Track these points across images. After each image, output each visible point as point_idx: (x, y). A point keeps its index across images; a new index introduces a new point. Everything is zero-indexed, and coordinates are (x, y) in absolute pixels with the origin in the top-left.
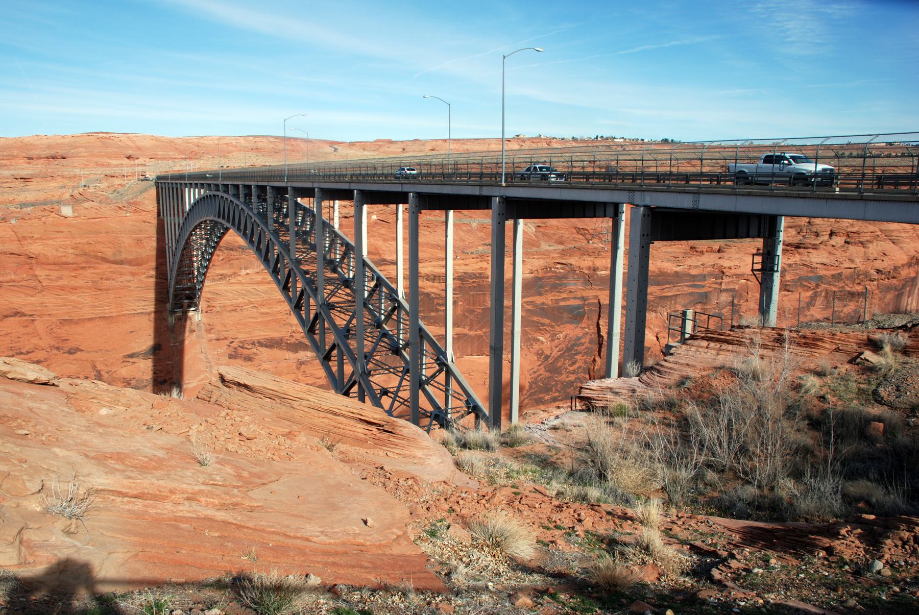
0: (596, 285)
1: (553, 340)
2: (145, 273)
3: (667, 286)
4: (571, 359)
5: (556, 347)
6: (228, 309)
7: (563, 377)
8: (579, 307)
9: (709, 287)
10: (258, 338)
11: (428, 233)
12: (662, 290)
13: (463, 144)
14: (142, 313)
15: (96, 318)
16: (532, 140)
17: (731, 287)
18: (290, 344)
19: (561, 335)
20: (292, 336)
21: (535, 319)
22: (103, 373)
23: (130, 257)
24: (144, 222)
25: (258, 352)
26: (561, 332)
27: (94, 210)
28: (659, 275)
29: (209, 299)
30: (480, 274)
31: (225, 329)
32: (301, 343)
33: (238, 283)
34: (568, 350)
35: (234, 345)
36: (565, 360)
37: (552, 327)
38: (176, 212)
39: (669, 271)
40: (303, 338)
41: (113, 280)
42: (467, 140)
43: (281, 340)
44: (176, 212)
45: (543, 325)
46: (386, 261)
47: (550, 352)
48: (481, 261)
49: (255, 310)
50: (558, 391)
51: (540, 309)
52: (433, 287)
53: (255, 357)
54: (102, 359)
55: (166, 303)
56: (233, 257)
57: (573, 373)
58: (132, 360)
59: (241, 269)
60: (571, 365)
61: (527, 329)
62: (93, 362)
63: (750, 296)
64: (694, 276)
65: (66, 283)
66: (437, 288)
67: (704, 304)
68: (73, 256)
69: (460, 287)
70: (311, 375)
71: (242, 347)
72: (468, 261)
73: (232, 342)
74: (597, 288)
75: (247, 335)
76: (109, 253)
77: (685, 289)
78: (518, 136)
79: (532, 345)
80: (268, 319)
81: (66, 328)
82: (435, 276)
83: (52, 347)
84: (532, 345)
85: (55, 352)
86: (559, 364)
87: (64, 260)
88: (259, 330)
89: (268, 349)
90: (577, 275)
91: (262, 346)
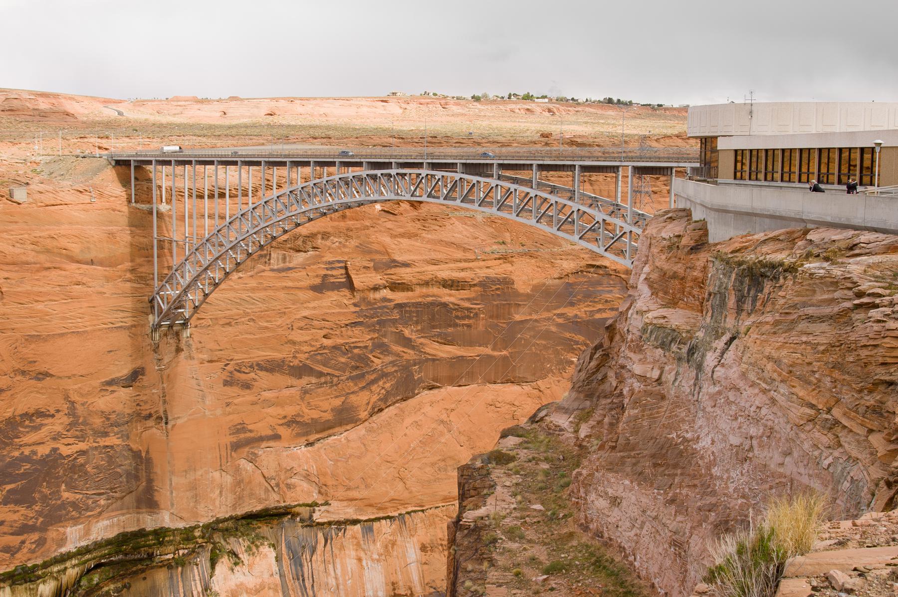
2: (120, 277)
6: (221, 323)
10: (257, 359)
11: (438, 227)
15: (68, 333)
18: (292, 367)
20: (295, 357)
21: (568, 335)
24: (114, 210)
30: (505, 278)
31: (219, 348)
32: (305, 365)
33: (231, 290)
40: (307, 359)
41: (84, 284)
43: (283, 362)
45: (577, 343)
48: (505, 262)
49: (251, 323)
52: (450, 295)
53: (253, 383)
54: (76, 387)
58: (110, 389)
61: (559, 348)
62: (66, 390)
65: (29, 288)
68: (33, 253)
69: (482, 295)
70: (317, 407)
71: (239, 371)
72: (490, 263)
73: (226, 365)
75: (249, 356)
76: (75, 248)
79: (564, 369)
80: (268, 335)
81: (33, 346)
82: (453, 281)
83: (17, 372)
85: (19, 378)
87: (24, 258)
88: (258, 349)
91: (261, 370)
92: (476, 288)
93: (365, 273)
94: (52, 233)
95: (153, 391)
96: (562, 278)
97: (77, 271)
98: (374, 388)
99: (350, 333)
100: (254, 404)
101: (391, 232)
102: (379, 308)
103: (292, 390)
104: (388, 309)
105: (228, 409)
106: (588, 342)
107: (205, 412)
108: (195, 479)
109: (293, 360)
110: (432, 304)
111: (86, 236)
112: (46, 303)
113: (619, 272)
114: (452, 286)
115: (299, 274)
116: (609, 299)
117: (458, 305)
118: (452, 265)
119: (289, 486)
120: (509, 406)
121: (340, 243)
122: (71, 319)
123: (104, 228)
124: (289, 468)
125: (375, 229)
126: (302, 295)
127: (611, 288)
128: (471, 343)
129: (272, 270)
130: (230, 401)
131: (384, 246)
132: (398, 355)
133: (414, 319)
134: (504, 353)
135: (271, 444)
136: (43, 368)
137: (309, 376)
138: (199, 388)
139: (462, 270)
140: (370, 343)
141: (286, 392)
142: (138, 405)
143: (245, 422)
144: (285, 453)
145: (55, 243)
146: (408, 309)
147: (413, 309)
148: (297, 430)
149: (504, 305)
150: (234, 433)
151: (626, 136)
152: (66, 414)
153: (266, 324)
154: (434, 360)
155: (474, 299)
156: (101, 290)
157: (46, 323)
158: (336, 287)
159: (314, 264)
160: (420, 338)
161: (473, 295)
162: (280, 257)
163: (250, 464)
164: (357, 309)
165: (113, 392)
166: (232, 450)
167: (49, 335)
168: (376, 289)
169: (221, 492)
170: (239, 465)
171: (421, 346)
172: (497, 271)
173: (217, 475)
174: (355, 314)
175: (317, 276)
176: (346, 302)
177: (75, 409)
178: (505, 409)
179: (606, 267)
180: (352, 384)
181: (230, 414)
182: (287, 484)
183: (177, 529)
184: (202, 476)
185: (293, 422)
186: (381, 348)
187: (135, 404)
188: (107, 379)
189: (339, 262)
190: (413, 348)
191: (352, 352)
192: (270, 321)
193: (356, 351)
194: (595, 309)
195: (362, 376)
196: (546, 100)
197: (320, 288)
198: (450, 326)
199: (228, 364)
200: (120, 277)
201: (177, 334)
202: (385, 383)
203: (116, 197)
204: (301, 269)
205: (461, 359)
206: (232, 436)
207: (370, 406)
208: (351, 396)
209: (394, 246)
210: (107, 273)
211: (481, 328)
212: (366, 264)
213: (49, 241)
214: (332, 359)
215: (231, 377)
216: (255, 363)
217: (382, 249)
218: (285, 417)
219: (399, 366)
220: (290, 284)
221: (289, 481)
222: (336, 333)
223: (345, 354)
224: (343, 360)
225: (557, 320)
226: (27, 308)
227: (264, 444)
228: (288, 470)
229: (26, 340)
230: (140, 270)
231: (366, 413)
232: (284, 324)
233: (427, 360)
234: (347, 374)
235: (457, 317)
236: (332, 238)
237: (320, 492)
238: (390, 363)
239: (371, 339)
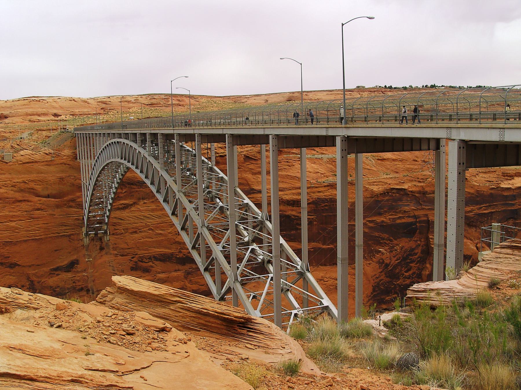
0: (426, 206)
1: (391, 252)
2: (66, 205)
4: (406, 267)
5: (394, 257)
6: (130, 231)
8: (411, 224)
14: (64, 235)
15: (29, 239)
16: (371, 90)
20: (180, 252)
22: (36, 283)
23: (54, 192)
24: (65, 164)
26: (397, 245)
27: (28, 156)
29: (115, 223)
31: (128, 247)
33: (137, 211)
34: (404, 259)
37: (391, 241)
38: (89, 156)
43: (172, 255)
44: (89, 156)
45: (383, 239)
46: (255, 190)
48: (331, 188)
51: (380, 226)
52: (292, 210)
54: (34, 272)
55: (82, 227)
56: (133, 190)
57: (409, 278)
58: (57, 273)
59: (139, 199)
60: (406, 272)
61: (370, 242)
62: (28, 274)
67: (516, 219)
68: (12, 192)
69: (314, 209)
70: (196, 283)
73: (132, 258)
74: (427, 208)
76: (38, 188)
78: (358, 87)
81: (7, 248)
84: (374, 256)
86: (397, 271)
87: (6, 195)
88: (154, 247)
89: (161, 263)
91: (157, 261)
94: (25, 179)
95: (84, 274)
96: (373, 197)
97: (39, 202)
101: (253, 171)
103: (179, 273)
106: (392, 238)
109: (179, 254)
111: (46, 180)
112: (17, 222)
113: (414, 193)
114: (294, 204)
116: (406, 210)
117: (298, 217)
118: (294, 191)
120: (334, 280)
122: (32, 231)
123: (58, 175)
125: (241, 170)
127: (408, 203)
131: (246, 180)
136: (14, 260)
137: (190, 263)
141: (175, 274)
142: (74, 282)
145: (26, 186)
149: (330, 215)
152: (28, 288)
153: (160, 232)
156: (53, 213)
157: (16, 234)
165: (58, 275)
167: (17, 241)
172: (325, 194)
177: (34, 285)
178: (330, 283)
179: (405, 189)
187: (72, 282)
188: (54, 267)
192: (164, 230)
196: (443, 88)
199: (134, 257)
200: (66, 205)
201: (101, 239)
203: (68, 156)
209: (253, 180)
210: (57, 203)
213: (22, 184)
217: (245, 182)
225: (369, 224)
226: (5, 225)
229: (4, 244)
230: (78, 200)
232: (173, 231)
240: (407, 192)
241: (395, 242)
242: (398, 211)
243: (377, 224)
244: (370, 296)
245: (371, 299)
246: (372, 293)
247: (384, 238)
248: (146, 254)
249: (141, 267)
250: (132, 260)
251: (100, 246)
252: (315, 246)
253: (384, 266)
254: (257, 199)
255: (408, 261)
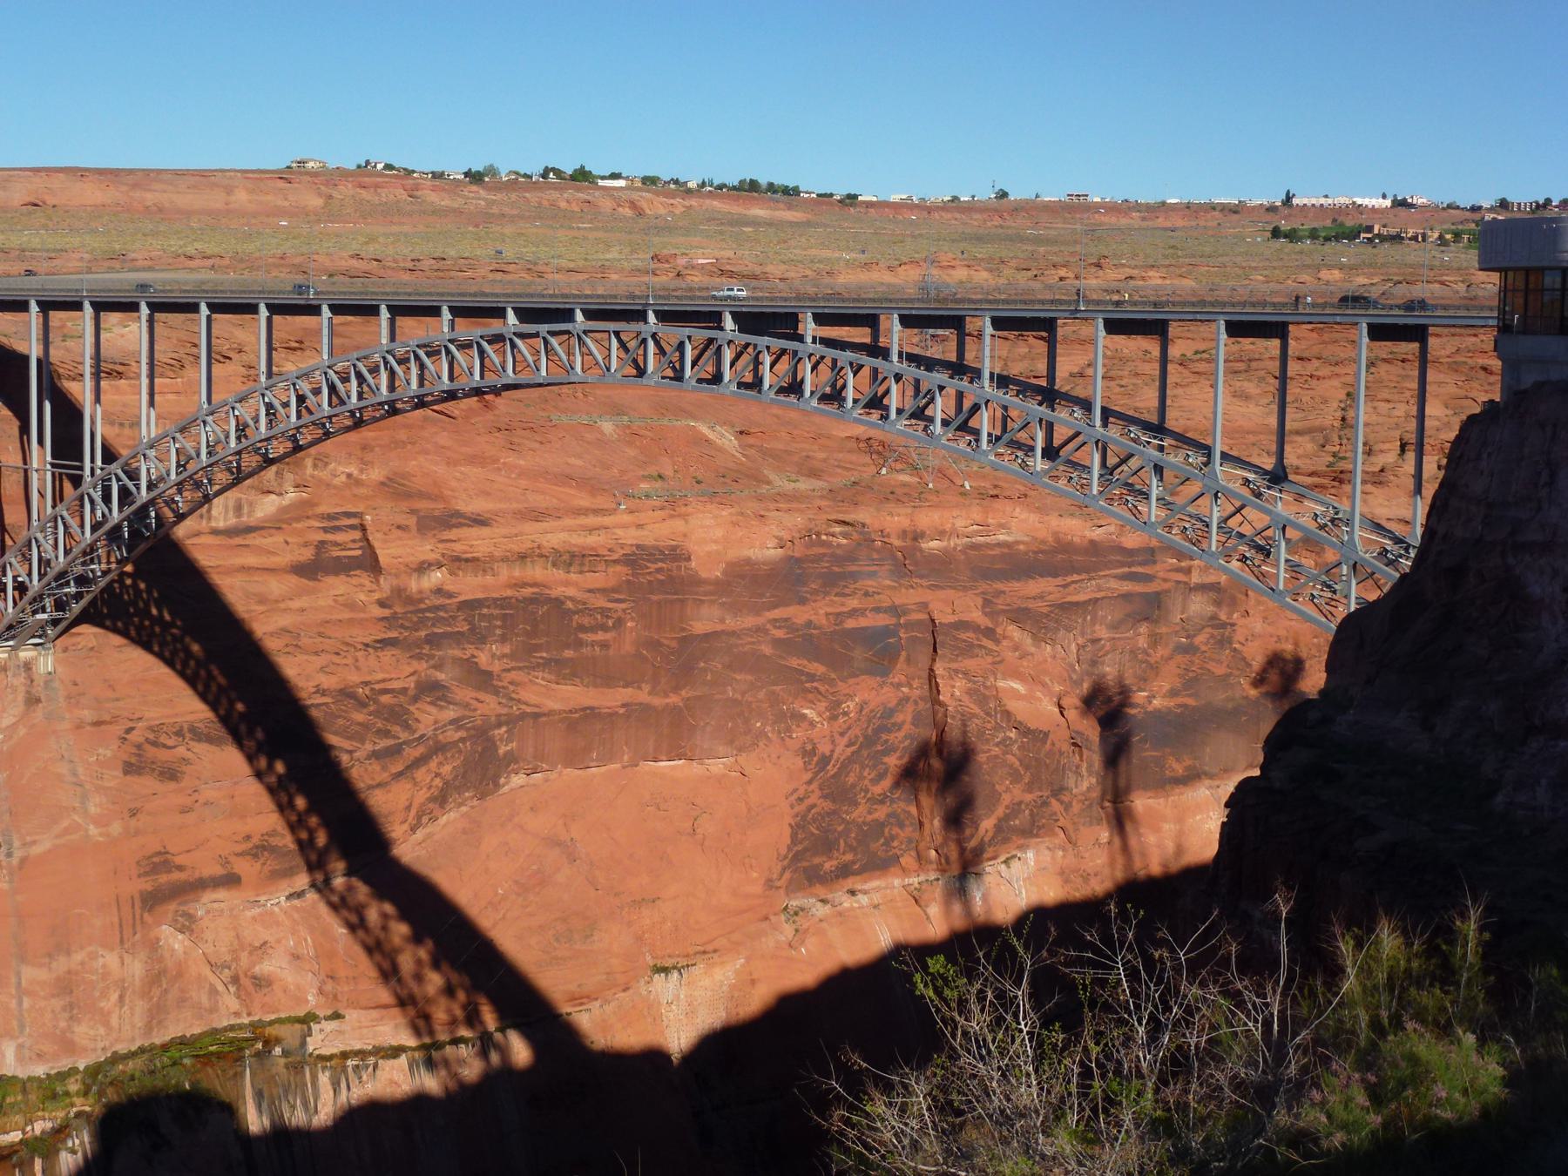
0: (921, 577)
1: (834, 718)
3: (1076, 577)
4: (875, 766)
5: (842, 734)
7: (859, 813)
8: (887, 632)
9: (1165, 580)
10: (190, 718)
11: (537, 445)
12: (1064, 586)
13: (135, 186)
17: (1211, 579)
19: (851, 705)
21: (794, 662)
25: (189, 755)
26: (850, 697)
28: (1055, 551)
30: (674, 548)
34: (869, 741)
35: (136, 737)
36: (863, 767)
37: (831, 682)
39: (1076, 540)
42: (147, 172)
45: (812, 677)
47: (831, 747)
48: (672, 516)
50: (852, 849)
52: (567, 583)
53: (184, 768)
57: (882, 802)
61: (777, 688)
63: (1252, 602)
64: (1130, 552)
66: (576, 584)
69: (628, 581)
71: (155, 744)
72: (643, 517)
73: (129, 730)
74: (925, 582)
77: (1113, 584)
78: (302, 162)
79: (789, 730)
82: (573, 556)
86: (851, 779)
89: (213, 748)
90: (878, 551)
91: (199, 741)
92: (619, 568)
93: (400, 539)
98: (421, 774)
99: (372, 661)
100: (185, 810)
102: (429, 609)
104: (446, 612)
105: (133, 822)
107: (87, 830)
108: (69, 972)
110: (532, 600)
114: (570, 565)
115: (269, 540)
116: (871, 590)
117: (584, 604)
118: (568, 522)
119: (261, 983)
121: (349, 476)
124: (257, 945)
126: (276, 586)
128: (607, 679)
129: (215, 532)
130: (138, 805)
132: (467, 706)
133: (498, 632)
134: (673, 699)
135: (221, 894)
138: (74, 780)
139: (591, 530)
140: (411, 683)
143: (170, 849)
144: (249, 914)
146: (485, 611)
147: (496, 612)
148: (273, 864)
149: (672, 602)
150: (146, 874)
151: (820, 261)
154: (536, 716)
155: (614, 590)
158: (342, 567)
159: (298, 519)
160: (508, 670)
161: (612, 583)
162: (231, 504)
163: (180, 937)
164: (386, 612)
166: (143, 908)
168: (423, 568)
169: (121, 997)
170: (158, 940)
171: (512, 688)
173: (111, 959)
174: (383, 624)
175: (306, 545)
176: (362, 597)
179: (864, 525)
180: (378, 768)
181: (137, 833)
182: (255, 978)
183: (30, 1079)
184: (82, 963)
185: (264, 848)
186: (431, 690)
189: (348, 515)
190: (496, 692)
191: (376, 702)
193: (385, 699)
194: (845, 610)
195: (395, 751)
196: (621, 183)
197: (312, 569)
198: (567, 646)
199: (132, 729)
201: (28, 666)
202: (440, 764)
204: (273, 531)
205: (590, 713)
206: (143, 879)
207: (413, 812)
208: (377, 792)
211: (628, 647)
212: (402, 519)
214: (340, 717)
215: (139, 755)
216: (186, 729)
218: (248, 837)
219: (468, 730)
220: (251, 560)
221: (257, 970)
222: (344, 661)
223: (363, 705)
224: (359, 717)
227: (208, 896)
228: (256, 949)
231: (406, 827)
233: (523, 716)
234: (369, 747)
235: (582, 628)
236: (332, 466)
237: (321, 992)
238: (453, 722)
239: (412, 674)
240: (869, 533)
241: (842, 687)
242: (847, 591)
243: (797, 630)
244: (786, 857)
245: (789, 867)
246: (789, 849)
247: (814, 675)
248: (168, 717)
249: (153, 763)
250: (125, 739)
251: (28, 692)
252: (630, 700)
253: (817, 764)
254: (471, 546)
255: (879, 748)
